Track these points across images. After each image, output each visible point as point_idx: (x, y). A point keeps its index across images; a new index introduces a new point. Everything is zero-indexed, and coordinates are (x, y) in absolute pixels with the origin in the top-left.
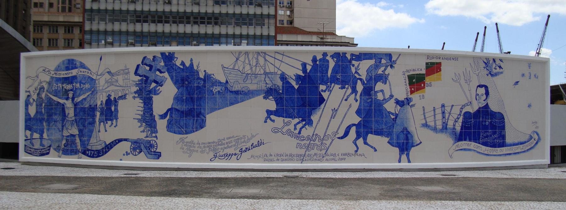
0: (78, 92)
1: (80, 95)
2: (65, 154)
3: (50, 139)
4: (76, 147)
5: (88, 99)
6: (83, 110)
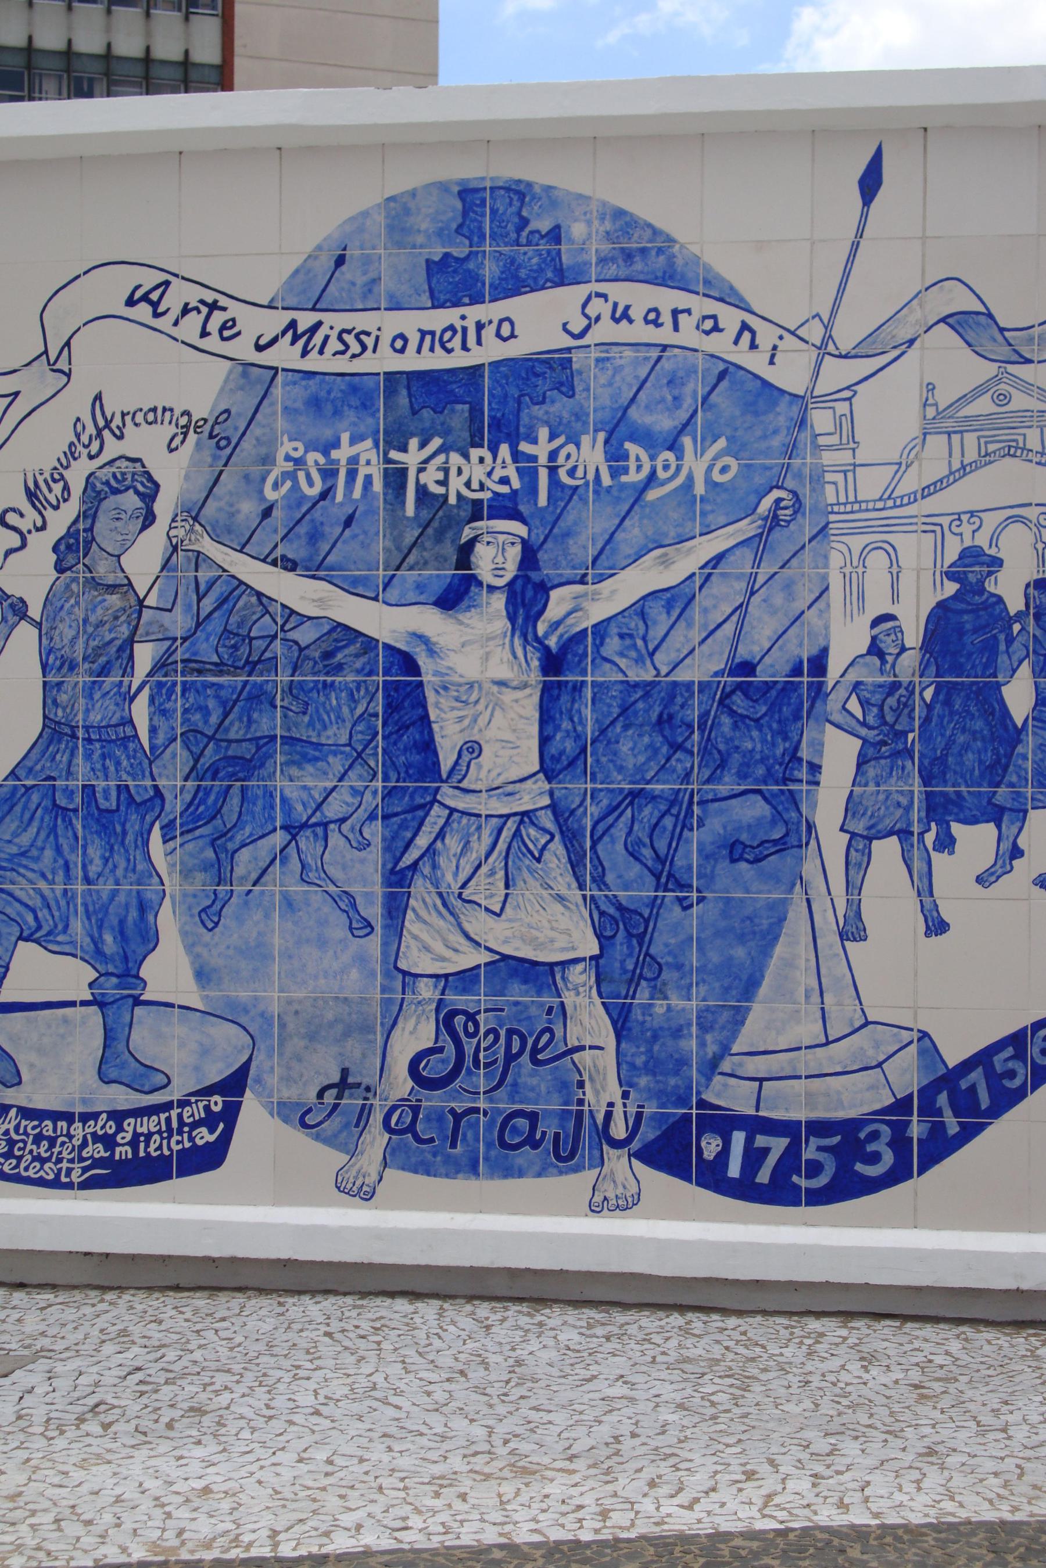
0: (591, 524)
1: (603, 564)
2: (425, 1168)
3: (229, 1014)
4: (571, 1087)
5: (720, 599)
6: (660, 710)
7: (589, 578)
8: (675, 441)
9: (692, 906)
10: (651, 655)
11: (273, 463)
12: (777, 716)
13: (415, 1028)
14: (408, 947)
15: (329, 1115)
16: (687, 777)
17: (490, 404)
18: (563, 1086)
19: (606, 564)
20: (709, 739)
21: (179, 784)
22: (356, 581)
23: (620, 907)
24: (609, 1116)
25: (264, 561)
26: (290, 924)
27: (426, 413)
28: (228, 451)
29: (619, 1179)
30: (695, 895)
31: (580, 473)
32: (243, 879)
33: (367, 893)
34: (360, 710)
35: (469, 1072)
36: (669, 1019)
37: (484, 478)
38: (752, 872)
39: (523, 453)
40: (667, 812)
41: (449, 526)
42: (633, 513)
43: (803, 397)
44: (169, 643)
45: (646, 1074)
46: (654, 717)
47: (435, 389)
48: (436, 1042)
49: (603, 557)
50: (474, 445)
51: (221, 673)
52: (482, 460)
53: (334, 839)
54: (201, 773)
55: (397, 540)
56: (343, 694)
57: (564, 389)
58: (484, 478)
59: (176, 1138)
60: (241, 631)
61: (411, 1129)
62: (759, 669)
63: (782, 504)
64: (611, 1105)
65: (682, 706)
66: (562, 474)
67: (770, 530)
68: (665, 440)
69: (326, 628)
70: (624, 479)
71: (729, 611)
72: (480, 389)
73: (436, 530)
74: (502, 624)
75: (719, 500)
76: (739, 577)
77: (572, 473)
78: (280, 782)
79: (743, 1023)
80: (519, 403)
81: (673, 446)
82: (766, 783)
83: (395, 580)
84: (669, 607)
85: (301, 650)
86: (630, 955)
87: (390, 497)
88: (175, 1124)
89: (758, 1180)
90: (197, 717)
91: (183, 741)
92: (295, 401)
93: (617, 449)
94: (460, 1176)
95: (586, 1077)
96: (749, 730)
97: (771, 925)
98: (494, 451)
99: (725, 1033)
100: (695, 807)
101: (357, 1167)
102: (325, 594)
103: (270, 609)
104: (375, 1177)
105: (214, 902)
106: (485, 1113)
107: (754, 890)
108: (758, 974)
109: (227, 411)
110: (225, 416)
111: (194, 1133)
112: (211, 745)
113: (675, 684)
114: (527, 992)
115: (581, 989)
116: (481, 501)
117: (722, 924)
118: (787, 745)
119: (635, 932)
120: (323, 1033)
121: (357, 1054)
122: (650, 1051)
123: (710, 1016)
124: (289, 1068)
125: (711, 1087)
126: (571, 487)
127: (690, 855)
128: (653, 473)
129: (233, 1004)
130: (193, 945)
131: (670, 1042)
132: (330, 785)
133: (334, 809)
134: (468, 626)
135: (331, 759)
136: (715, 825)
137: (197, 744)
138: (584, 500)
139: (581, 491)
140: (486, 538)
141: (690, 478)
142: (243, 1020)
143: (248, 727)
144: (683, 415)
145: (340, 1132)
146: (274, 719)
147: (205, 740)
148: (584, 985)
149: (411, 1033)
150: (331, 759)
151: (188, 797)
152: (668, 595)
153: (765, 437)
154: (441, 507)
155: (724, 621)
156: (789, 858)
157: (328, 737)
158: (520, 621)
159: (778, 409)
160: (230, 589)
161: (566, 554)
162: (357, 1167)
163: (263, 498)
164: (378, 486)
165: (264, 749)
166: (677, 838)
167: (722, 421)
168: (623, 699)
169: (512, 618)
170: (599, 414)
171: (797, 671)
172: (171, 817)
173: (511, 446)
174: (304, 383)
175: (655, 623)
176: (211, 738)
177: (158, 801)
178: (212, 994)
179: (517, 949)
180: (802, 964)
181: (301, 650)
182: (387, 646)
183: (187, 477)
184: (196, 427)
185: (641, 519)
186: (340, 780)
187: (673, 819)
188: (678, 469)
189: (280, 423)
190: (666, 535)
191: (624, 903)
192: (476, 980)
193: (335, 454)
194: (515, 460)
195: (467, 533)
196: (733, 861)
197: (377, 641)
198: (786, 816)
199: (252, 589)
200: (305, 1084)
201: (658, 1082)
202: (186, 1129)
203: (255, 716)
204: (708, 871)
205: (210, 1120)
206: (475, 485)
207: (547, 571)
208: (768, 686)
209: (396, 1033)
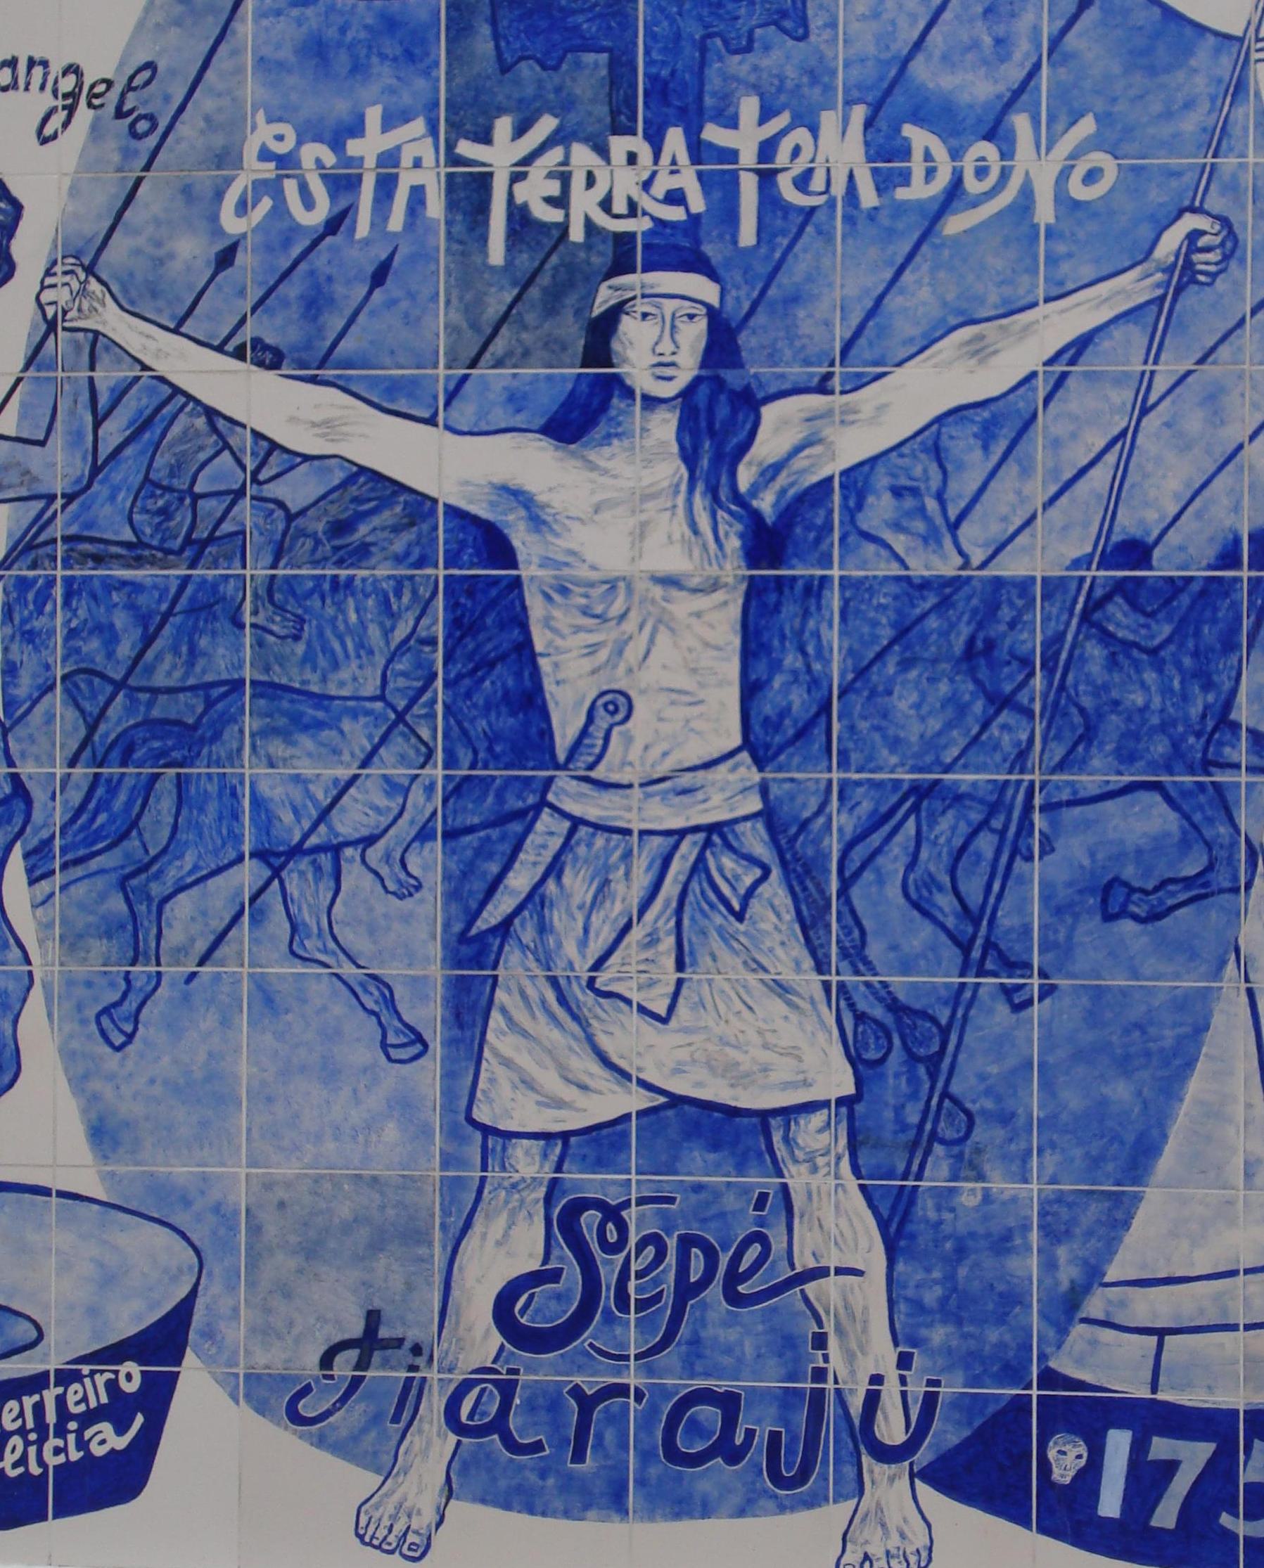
0: (840, 279)
1: (863, 355)
2: (526, 1501)
3: (155, 1208)
4: (801, 1346)
5: (1081, 423)
6: (973, 631)
7: (836, 383)
8: (998, 121)
9: (1029, 1003)
10: (954, 527)
11: (238, 164)
12: (1190, 644)
13: (506, 1235)
14: (492, 1081)
15: (344, 1399)
16: (1021, 758)
17: (647, 52)
18: (787, 1344)
19: (867, 356)
20: (1062, 687)
21: (59, 771)
22: (394, 387)
23: (895, 1006)
24: (872, 1400)
25: (220, 349)
26: (268, 1038)
27: (527, 70)
28: (152, 141)
29: (893, 1520)
30: (1036, 982)
31: (818, 183)
32: (180, 952)
33: (415, 979)
34: (401, 632)
35: (609, 1318)
36: (986, 1218)
37: (637, 193)
38: (1145, 939)
39: (710, 145)
40: (984, 825)
41: (570, 284)
42: (918, 259)
43: (1241, 40)
44: (40, 504)
45: (944, 1322)
46: (959, 645)
47: (544, 24)
48: (546, 1260)
49: (862, 341)
50: (617, 130)
51: (139, 562)
52: (632, 159)
53: (354, 875)
54: (100, 752)
55: (472, 311)
56: (370, 602)
57: (788, 24)
58: (637, 193)
59: (53, 1442)
60: (175, 483)
61: (499, 1425)
62: (1157, 553)
63: (1202, 242)
64: (877, 1379)
65: (1012, 625)
66: (785, 185)
67: (1179, 290)
68: (980, 121)
69: (338, 477)
70: (902, 194)
71: (1101, 443)
72: (628, 24)
73: (545, 290)
74: (671, 469)
75: (1081, 235)
76: (1119, 380)
77: (802, 182)
78: (249, 768)
79: (1126, 1224)
80: (703, 50)
81: (996, 131)
82: (1171, 772)
83: (468, 387)
84: (986, 436)
85: (290, 517)
86: (914, 1096)
87: (457, 229)
88: (51, 1417)
89: (1155, 1522)
90: (93, 645)
91: (66, 691)
92: (278, 47)
93: (889, 138)
94: (591, 1514)
95: (829, 1328)
96: (1138, 671)
97: (1180, 1039)
98: (656, 140)
99: (1093, 1243)
100: (1036, 816)
101: (396, 1498)
102: (336, 413)
103: (232, 441)
104: (429, 1516)
105: (125, 995)
106: (639, 1396)
107: (1147, 970)
108: (1155, 1132)
109: (150, 66)
110: (146, 74)
111: (88, 1434)
112: (120, 698)
113: (998, 582)
114: (718, 1165)
115: (821, 1161)
116: (631, 236)
117: (1087, 1037)
118: (1211, 698)
119: (922, 1052)
120: (332, 1244)
121: (397, 1282)
122: (950, 1277)
123: (1064, 1213)
124: (268, 1311)
125: (1066, 1347)
126: (801, 210)
127: (1026, 910)
128: (957, 183)
129: (161, 1189)
130: (86, 1077)
131: (988, 1262)
132: (344, 773)
133: (351, 820)
134: (605, 472)
135: (347, 725)
136: (1075, 850)
137: (94, 696)
138: (826, 235)
139: (820, 217)
140: (641, 306)
141: (1027, 192)
142: (175, 1220)
143: (191, 664)
144: (1014, 73)
145: (364, 1430)
146: (239, 648)
147: (109, 689)
148: (826, 1153)
149: (499, 1244)
150: (347, 725)
151: (76, 797)
152: (986, 414)
153: (1168, 115)
154: (554, 248)
155: (1092, 464)
156: (1213, 912)
157: (342, 684)
158: (705, 462)
159: (1193, 63)
160: (155, 402)
161: (791, 337)
162: (396, 1498)
163: (218, 231)
164: (435, 207)
165: (220, 706)
166: (1003, 874)
167: (1088, 84)
168: (899, 612)
169: (689, 457)
170: (855, 72)
171: (1229, 557)
172: (45, 834)
173: (687, 133)
174: (295, 12)
175: (961, 466)
176: (119, 685)
177: (19, 805)
178: (121, 1169)
179: (699, 1084)
180: (1239, 1112)
181: (290, 517)
182: (454, 512)
183: (74, 191)
184: (92, 95)
185: (935, 268)
186: (365, 764)
187: (995, 839)
188: (1005, 175)
189: (251, 89)
190: (981, 301)
191: (901, 996)
192: (621, 1143)
193: (354, 147)
194: (696, 159)
195: (605, 297)
196: (1109, 917)
197: (435, 501)
198: (1208, 833)
199: (198, 402)
200: (297, 1341)
201: (965, 1336)
202: (73, 1425)
203: (204, 642)
204: (1061, 936)
205: (118, 1409)
206: (620, 206)
207: (756, 369)
208: (1175, 586)
209: (471, 1244)
